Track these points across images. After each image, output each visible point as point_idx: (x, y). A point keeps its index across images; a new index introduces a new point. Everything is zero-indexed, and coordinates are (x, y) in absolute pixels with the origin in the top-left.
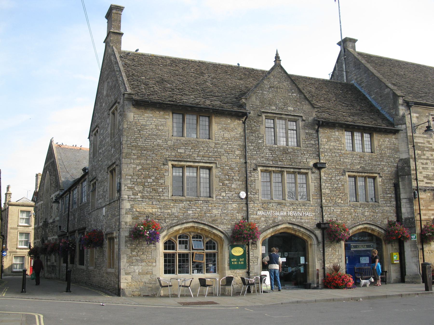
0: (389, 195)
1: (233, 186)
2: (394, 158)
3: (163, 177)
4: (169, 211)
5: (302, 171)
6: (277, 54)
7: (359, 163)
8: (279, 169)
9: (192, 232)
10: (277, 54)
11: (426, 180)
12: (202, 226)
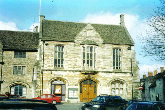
7: (19, 62)
11: (48, 67)
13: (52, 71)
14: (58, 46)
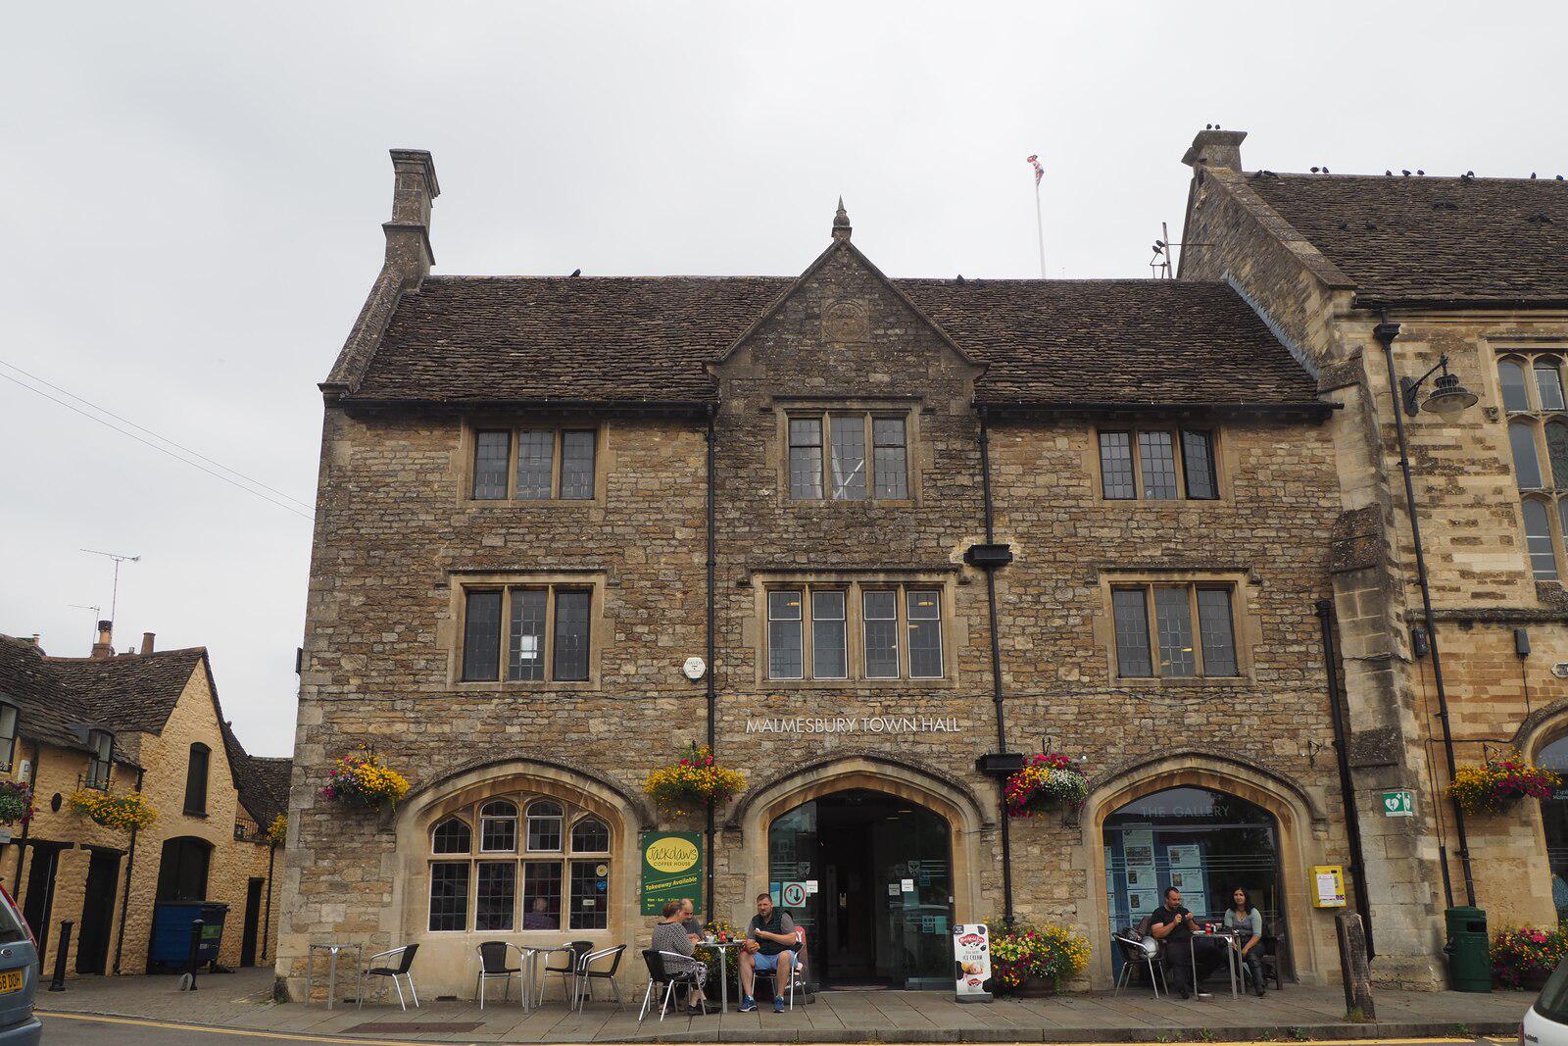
0: (1296, 648)
1: (664, 641)
2: (1317, 512)
3: (430, 624)
4: (446, 728)
5: (922, 578)
6: (841, 210)
7: (1158, 540)
8: (833, 578)
9: (527, 793)
10: (841, 210)
12: (551, 774)
13: (1531, 631)
14: (1531, 359)
